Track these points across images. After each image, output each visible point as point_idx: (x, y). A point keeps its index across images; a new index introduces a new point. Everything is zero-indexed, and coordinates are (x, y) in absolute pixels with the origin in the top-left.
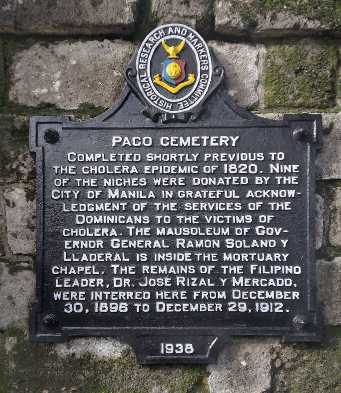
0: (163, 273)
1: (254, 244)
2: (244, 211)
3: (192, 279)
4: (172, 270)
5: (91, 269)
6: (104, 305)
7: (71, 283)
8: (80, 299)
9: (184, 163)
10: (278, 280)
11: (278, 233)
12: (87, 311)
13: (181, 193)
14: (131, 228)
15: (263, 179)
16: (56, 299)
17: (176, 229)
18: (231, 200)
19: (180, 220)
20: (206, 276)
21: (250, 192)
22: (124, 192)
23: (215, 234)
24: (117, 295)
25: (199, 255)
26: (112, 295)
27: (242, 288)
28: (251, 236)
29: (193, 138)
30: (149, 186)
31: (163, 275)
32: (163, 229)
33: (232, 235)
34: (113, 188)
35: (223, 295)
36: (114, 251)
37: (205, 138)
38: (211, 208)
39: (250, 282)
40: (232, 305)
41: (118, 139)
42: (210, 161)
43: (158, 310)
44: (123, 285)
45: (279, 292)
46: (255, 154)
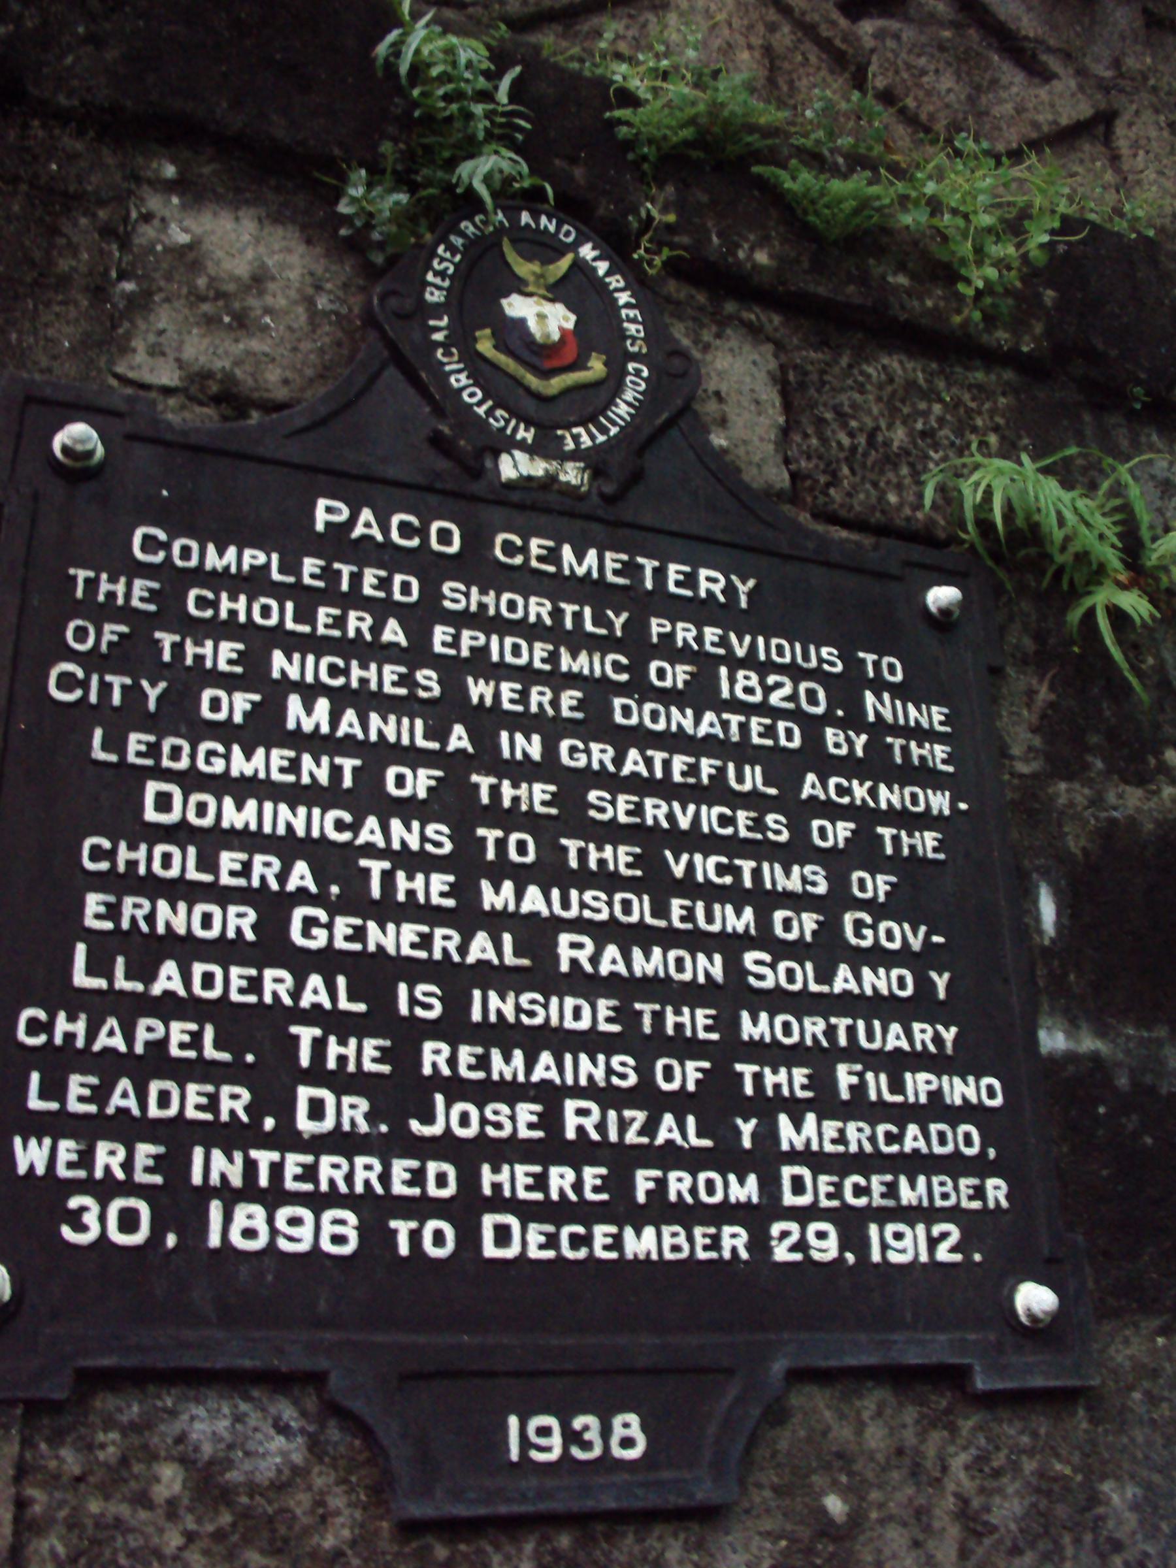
3: (628, 1114)
4: (545, 1068)
5: (196, 1040)
6: (250, 1217)
7: (100, 1095)
8: (141, 1177)
9: (578, 641)
11: (916, 944)
12: (171, 1240)
13: (573, 750)
14: (377, 867)
17: (555, 893)
18: (752, 800)
20: (680, 1103)
21: (811, 778)
22: (350, 715)
24: (310, 1173)
25: (646, 1009)
27: (816, 1161)
31: (511, 1092)
32: (508, 887)
33: (763, 938)
34: (310, 693)
35: (746, 1190)
38: (684, 823)
39: (841, 1139)
40: (785, 1234)
42: (668, 649)
43: (490, 1250)
44: (339, 1124)
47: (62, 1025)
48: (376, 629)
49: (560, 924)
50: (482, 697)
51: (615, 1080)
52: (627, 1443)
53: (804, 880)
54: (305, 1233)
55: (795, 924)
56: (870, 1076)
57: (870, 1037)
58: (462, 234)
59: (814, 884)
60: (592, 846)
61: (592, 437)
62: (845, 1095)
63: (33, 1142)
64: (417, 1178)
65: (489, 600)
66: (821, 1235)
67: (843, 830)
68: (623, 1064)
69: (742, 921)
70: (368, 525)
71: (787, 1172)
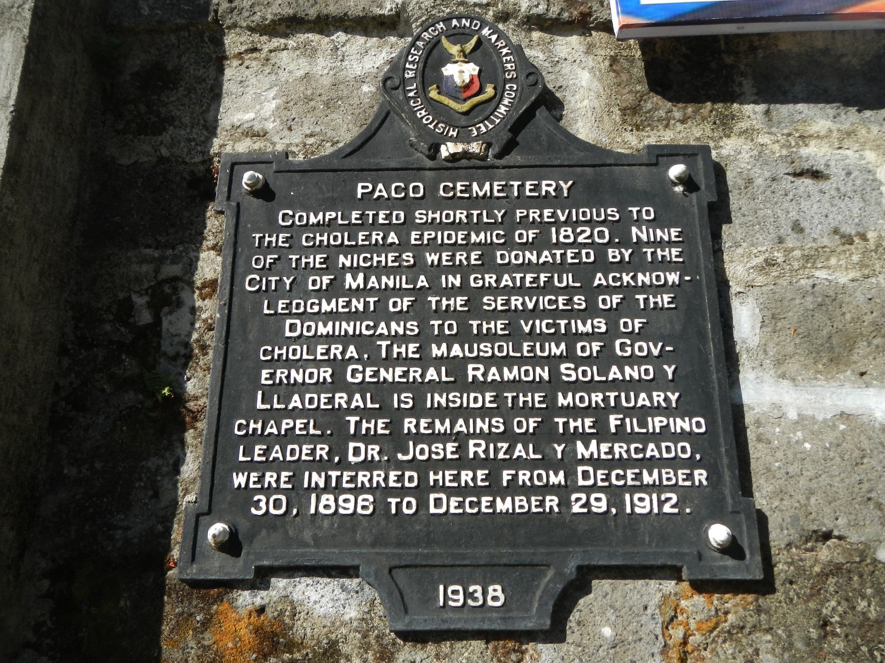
0: (442, 431)
1: (614, 373)
2: (590, 312)
3: (499, 445)
4: (460, 426)
5: (307, 425)
6: (327, 500)
7: (266, 452)
8: (283, 486)
9: (479, 227)
10: (663, 445)
11: (656, 352)
13: (476, 279)
14: (384, 344)
15: (621, 253)
16: (236, 486)
17: (466, 346)
19: (475, 327)
20: (525, 438)
21: (599, 275)
22: (373, 278)
23: (539, 353)
24: (353, 479)
26: (346, 478)
28: (605, 359)
29: (496, 183)
30: (419, 267)
32: (444, 346)
33: (570, 356)
35: (558, 479)
36: (350, 390)
37: (516, 184)
38: (530, 306)
39: (611, 451)
40: (578, 500)
41: (367, 187)
42: (525, 223)
43: (433, 510)
45: (668, 470)
46: (602, 210)
47: (252, 425)
48: (384, 238)
49: (466, 360)
50: (433, 261)
51: (494, 430)
52: (495, 598)
53: (593, 327)
54: (351, 506)
55: (588, 348)
56: (628, 420)
57: (628, 400)
58: (424, 40)
59: (599, 328)
60: (484, 323)
61: (486, 127)
62: (613, 430)
63: (240, 474)
64: (400, 479)
65: (437, 215)
66: (598, 500)
67: (616, 299)
68: (497, 422)
69: (558, 350)
70: (380, 191)
71: (580, 469)
